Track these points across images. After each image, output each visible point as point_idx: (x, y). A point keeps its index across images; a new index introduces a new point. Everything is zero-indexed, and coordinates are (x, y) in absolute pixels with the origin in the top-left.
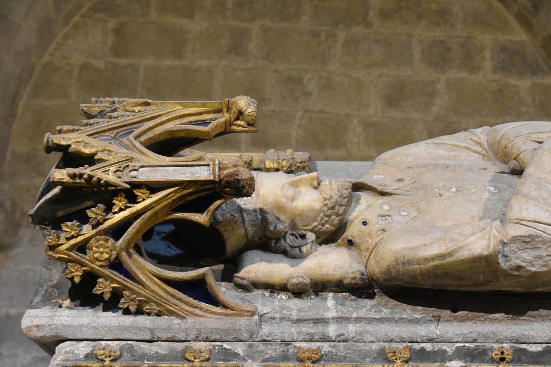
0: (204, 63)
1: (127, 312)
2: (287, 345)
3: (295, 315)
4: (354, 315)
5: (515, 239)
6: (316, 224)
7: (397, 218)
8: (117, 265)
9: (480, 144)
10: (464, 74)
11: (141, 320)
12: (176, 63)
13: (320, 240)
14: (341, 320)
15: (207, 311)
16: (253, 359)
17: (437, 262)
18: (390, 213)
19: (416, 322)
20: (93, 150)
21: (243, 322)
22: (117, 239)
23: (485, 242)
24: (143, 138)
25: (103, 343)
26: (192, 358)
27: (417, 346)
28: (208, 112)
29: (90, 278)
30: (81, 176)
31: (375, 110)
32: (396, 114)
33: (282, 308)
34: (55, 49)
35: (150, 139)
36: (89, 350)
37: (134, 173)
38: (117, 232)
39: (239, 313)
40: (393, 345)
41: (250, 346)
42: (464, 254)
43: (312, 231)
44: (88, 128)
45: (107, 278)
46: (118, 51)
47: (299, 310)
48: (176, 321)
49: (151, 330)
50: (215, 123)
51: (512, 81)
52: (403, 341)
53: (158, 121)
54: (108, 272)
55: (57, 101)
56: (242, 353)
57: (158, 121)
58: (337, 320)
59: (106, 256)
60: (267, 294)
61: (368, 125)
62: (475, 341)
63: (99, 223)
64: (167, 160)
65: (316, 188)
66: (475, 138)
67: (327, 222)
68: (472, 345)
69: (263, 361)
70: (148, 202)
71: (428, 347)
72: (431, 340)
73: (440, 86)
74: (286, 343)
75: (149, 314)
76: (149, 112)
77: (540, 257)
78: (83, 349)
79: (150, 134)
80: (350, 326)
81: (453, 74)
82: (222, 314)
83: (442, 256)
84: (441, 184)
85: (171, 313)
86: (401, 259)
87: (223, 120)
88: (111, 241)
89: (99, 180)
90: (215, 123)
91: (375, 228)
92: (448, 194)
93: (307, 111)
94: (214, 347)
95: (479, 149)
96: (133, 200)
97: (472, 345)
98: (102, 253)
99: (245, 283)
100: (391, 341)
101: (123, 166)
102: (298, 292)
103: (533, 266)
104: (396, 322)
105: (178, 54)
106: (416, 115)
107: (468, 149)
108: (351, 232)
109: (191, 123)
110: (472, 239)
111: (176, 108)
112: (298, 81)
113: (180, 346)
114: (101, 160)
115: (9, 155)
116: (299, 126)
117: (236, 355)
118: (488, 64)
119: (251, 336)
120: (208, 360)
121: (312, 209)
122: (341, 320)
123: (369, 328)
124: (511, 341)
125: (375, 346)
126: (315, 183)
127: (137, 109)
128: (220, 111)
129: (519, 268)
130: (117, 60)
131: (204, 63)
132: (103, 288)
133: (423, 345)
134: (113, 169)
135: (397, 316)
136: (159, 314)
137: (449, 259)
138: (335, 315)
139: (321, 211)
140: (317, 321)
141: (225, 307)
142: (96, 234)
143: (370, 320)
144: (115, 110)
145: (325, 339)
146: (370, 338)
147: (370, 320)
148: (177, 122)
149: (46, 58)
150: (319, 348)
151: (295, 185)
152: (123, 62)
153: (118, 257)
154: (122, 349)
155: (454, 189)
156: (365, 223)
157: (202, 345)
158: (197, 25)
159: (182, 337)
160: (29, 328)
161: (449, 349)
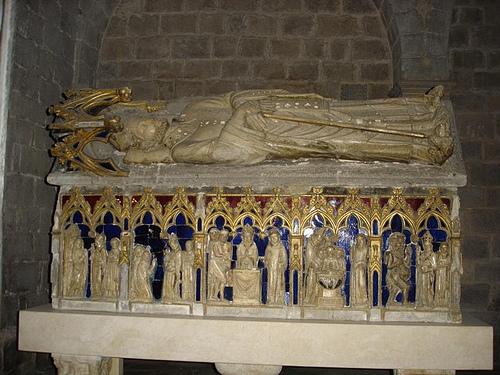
0: (192, 12)
10: (328, 13)
31: (280, 35)
32: (290, 36)
51: (353, 15)
61: (275, 42)
81: (321, 13)
106: (299, 36)
112: (240, 20)
118: (341, 6)
131: (192, 12)
149: (114, 15)
152: (152, 14)
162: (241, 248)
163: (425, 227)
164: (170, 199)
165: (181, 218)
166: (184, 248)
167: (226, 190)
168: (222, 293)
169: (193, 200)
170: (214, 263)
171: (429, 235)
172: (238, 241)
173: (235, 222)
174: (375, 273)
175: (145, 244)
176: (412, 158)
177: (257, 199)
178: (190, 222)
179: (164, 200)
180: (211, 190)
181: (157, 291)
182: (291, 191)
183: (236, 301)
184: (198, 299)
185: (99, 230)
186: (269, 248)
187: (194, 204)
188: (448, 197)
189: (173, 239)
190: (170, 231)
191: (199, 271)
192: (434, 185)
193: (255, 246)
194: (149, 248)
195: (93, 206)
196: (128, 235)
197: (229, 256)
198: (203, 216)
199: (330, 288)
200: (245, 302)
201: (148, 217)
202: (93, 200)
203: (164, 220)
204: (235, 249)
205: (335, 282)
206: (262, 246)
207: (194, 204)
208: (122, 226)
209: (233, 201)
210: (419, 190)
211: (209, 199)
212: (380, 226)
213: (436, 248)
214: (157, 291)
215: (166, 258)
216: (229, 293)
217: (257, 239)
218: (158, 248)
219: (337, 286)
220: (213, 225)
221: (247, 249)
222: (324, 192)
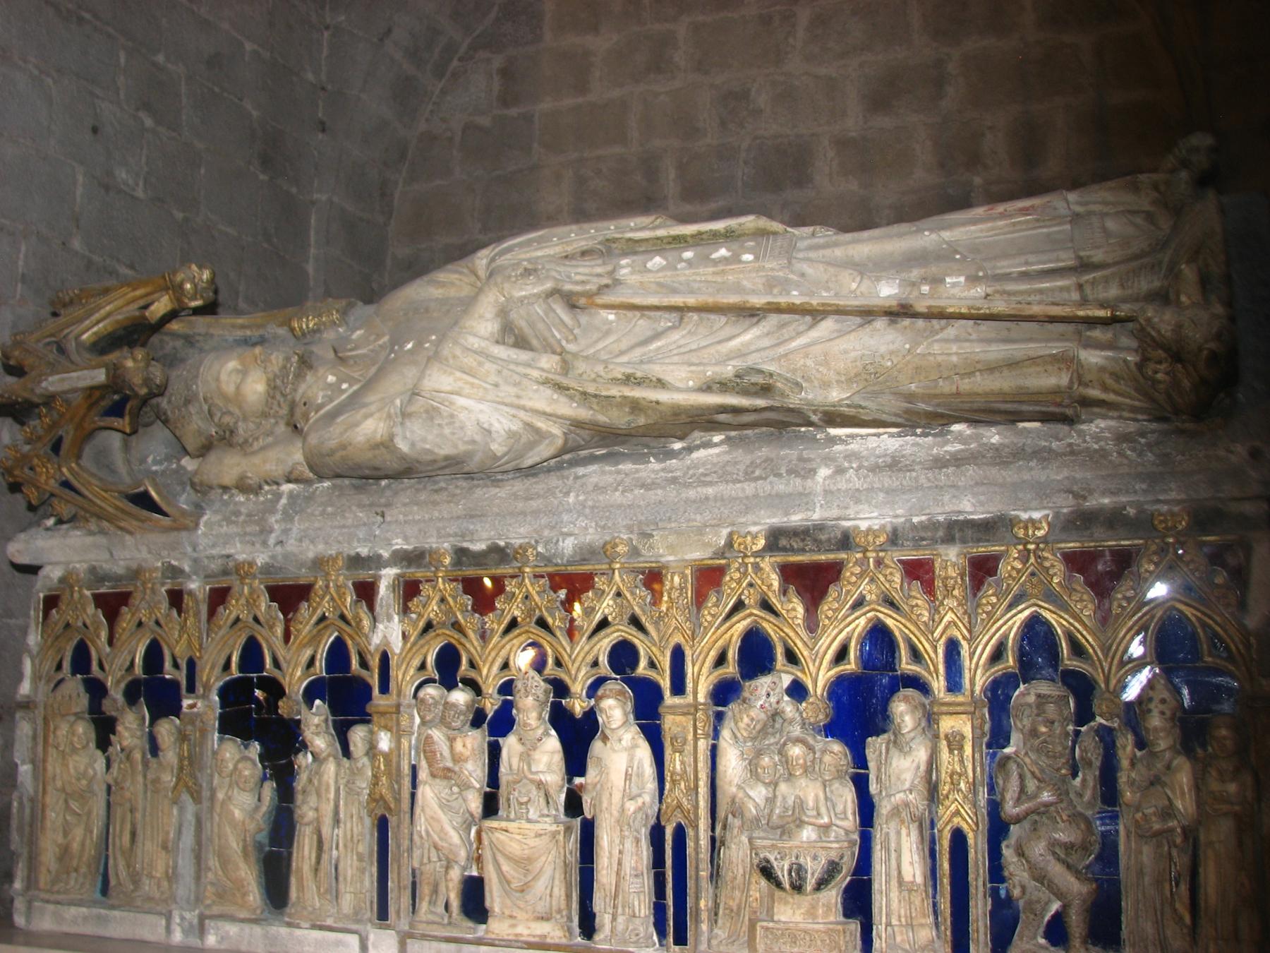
0: (616, 93)
12: (580, 100)
32: (884, 122)
34: (432, 111)
46: (506, 100)
55: (438, 182)
61: (842, 143)
73: (952, 68)
93: (756, 138)
105: (581, 87)
112: (744, 96)
115: (389, 262)
116: (746, 163)
130: (506, 112)
131: (616, 93)
149: (422, 126)
152: (513, 112)
158: (602, 43)
162: (510, 745)
169: (366, 592)
170: (428, 793)
172: (502, 723)
174: (958, 838)
176: (1086, 402)
179: (289, 596)
181: (277, 890)
182: (663, 551)
183: (497, 927)
184: (383, 914)
185: (132, 693)
186: (597, 746)
190: (311, 693)
196: (204, 706)
197: (475, 772)
198: (397, 645)
199: (798, 888)
200: (521, 929)
201: (252, 654)
202: (112, 604)
205: (814, 869)
206: (578, 736)
211: (410, 590)
214: (277, 890)
216: (474, 900)
217: (560, 719)
219: (821, 884)
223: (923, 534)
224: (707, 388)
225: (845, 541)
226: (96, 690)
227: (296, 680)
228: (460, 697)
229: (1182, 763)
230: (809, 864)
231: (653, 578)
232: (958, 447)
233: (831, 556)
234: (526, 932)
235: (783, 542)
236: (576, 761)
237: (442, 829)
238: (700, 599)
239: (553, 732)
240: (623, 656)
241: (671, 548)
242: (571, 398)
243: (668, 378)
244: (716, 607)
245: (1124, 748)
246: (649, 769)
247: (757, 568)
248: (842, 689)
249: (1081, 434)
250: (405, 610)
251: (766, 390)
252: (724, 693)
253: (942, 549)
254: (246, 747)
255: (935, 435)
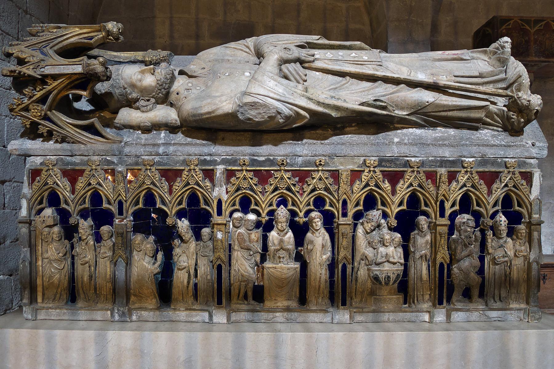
1: (57, 142)
2: (138, 157)
3: (143, 142)
4: (173, 142)
5: (246, 104)
6: (154, 94)
7: (194, 91)
8: (46, 118)
9: (248, 47)
11: (65, 145)
13: (160, 101)
14: (166, 144)
15: (98, 141)
16: (122, 165)
17: (207, 116)
18: (191, 88)
19: (204, 145)
20: (25, 56)
21: (115, 146)
22: (44, 104)
23: (231, 106)
24: (55, 48)
25: (48, 157)
26: (91, 165)
27: (202, 158)
28: (93, 32)
29: (35, 125)
30: (15, 71)
33: (138, 138)
35: (61, 48)
36: (41, 161)
37: (43, 70)
38: (43, 100)
39: (114, 142)
40: (191, 157)
41: (120, 158)
42: (220, 112)
43: (152, 97)
44: (26, 43)
45: (44, 125)
47: (146, 139)
48: (83, 146)
49: (70, 151)
50: (96, 38)
52: (196, 155)
53: (65, 37)
54: (42, 122)
56: (116, 162)
57: (65, 37)
58: (164, 144)
59: (40, 114)
60: (131, 131)
62: (232, 155)
63: (31, 97)
64: (66, 61)
65: (153, 74)
66: (246, 44)
67: (159, 92)
68: (230, 157)
69: (126, 165)
70: (54, 85)
71: (208, 158)
72: (211, 155)
74: (137, 156)
75: (69, 143)
76: (60, 32)
77: (260, 114)
78: (39, 160)
79: (60, 45)
80: (171, 147)
82: (105, 142)
83: (209, 113)
84: (222, 71)
85: (79, 142)
86: (190, 114)
87: (101, 36)
88: (41, 106)
89: (25, 73)
90: (96, 38)
91: (182, 97)
92: (223, 77)
94: (102, 159)
95: (248, 50)
96: (46, 84)
97: (230, 157)
98: (37, 112)
99: (118, 125)
100: (190, 155)
101: (37, 66)
102: (146, 130)
103: (257, 118)
104: (194, 145)
107: (242, 50)
108: (173, 98)
109: (85, 38)
110: (224, 103)
111: (77, 30)
113: (86, 158)
114: (29, 62)
117: (113, 163)
119: (120, 153)
120: (99, 165)
121: (151, 86)
122: (166, 144)
123: (180, 148)
124: (250, 155)
125: (181, 158)
126: (152, 71)
127: (55, 30)
128: (100, 31)
129: (249, 119)
132: (42, 130)
133: (205, 157)
134: (31, 67)
135: (194, 143)
136: (73, 143)
137: (213, 115)
138: (163, 142)
139: (156, 87)
140: (154, 145)
141: (107, 139)
142: (32, 102)
143: (181, 144)
144: (43, 31)
145: (158, 154)
146: (180, 154)
147: (181, 144)
148: (77, 38)
150: (153, 159)
151: (142, 72)
153: (46, 114)
154: (57, 160)
155: (227, 74)
156: (178, 94)
157: (96, 158)
159: (86, 154)
160: (11, 150)
161: (218, 159)
162: (273, 235)
163: (499, 207)
164: (178, 173)
165: (193, 199)
166: (198, 236)
167: (254, 162)
168: (250, 294)
169: (209, 174)
170: (238, 254)
171: (503, 218)
172: (268, 227)
173: (265, 200)
174: (442, 265)
175: (148, 234)
177: (295, 173)
178: (207, 203)
179: (170, 175)
180: (234, 162)
185: (84, 214)
186: (309, 235)
187: (212, 180)
188: (528, 170)
189: (184, 225)
191: (219, 268)
192: (511, 153)
193: (290, 234)
194: (152, 238)
195: (73, 182)
198: (225, 197)
201: (150, 198)
202: (73, 175)
203: (170, 200)
204: (265, 238)
206: (300, 231)
207: (212, 180)
208: (114, 209)
209: (263, 177)
210: (494, 162)
211: (230, 174)
212: (447, 205)
213: (511, 233)
215: (177, 251)
217: (293, 225)
218: (166, 239)
220: (237, 207)
221: (281, 237)
222: (380, 165)
223: (432, 164)
224: (362, 104)
225: (407, 164)
226: (64, 215)
227: (172, 210)
228: (252, 217)
229: (509, 240)
230: (392, 276)
231: (335, 175)
232: (441, 135)
233: (401, 169)
234: (281, 305)
235: (383, 164)
236: (300, 240)
237: (246, 268)
238: (352, 183)
239: (290, 230)
240: (319, 202)
241: (341, 164)
242: (314, 103)
243: (347, 100)
244: (357, 186)
245: (490, 235)
246: (329, 244)
247: (374, 172)
248: (399, 216)
249: (480, 133)
250: (228, 181)
251: (384, 108)
252: (358, 216)
253: (439, 169)
254: (147, 238)
255: (432, 130)
